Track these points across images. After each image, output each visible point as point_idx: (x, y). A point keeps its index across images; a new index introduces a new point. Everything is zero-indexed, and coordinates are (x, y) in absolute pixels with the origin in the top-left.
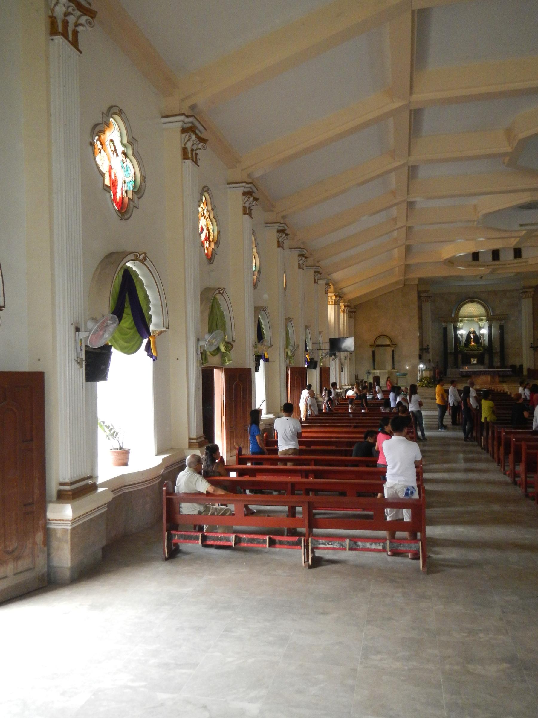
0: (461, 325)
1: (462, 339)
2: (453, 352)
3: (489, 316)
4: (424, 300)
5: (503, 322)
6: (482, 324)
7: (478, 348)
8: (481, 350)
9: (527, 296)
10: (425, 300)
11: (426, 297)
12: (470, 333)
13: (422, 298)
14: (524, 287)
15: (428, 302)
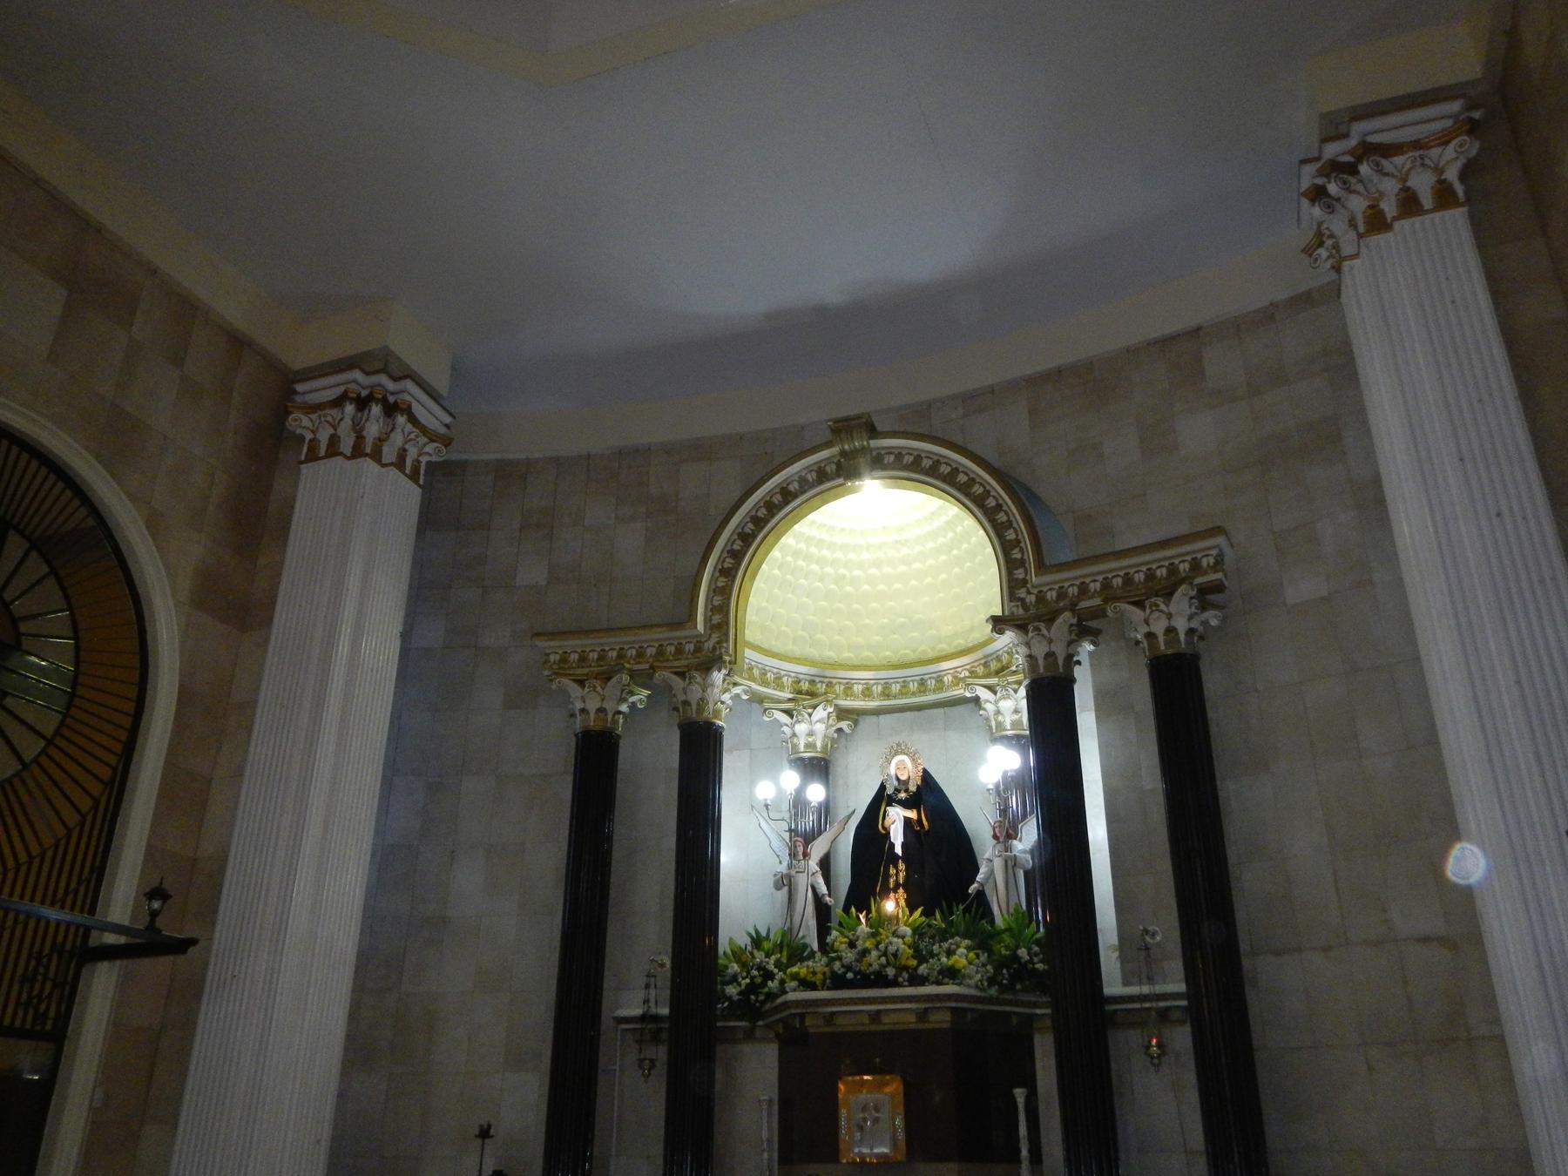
0: (801, 728)
1: (790, 866)
2: (665, 1011)
3: (1024, 582)
4: (324, 437)
5: (1180, 613)
6: (1007, 705)
7: (921, 957)
8: (952, 974)
9: (1389, 208)
10: (334, 441)
11: (338, 402)
12: (882, 799)
13: (300, 423)
14: (1333, 128)
15: (358, 452)
